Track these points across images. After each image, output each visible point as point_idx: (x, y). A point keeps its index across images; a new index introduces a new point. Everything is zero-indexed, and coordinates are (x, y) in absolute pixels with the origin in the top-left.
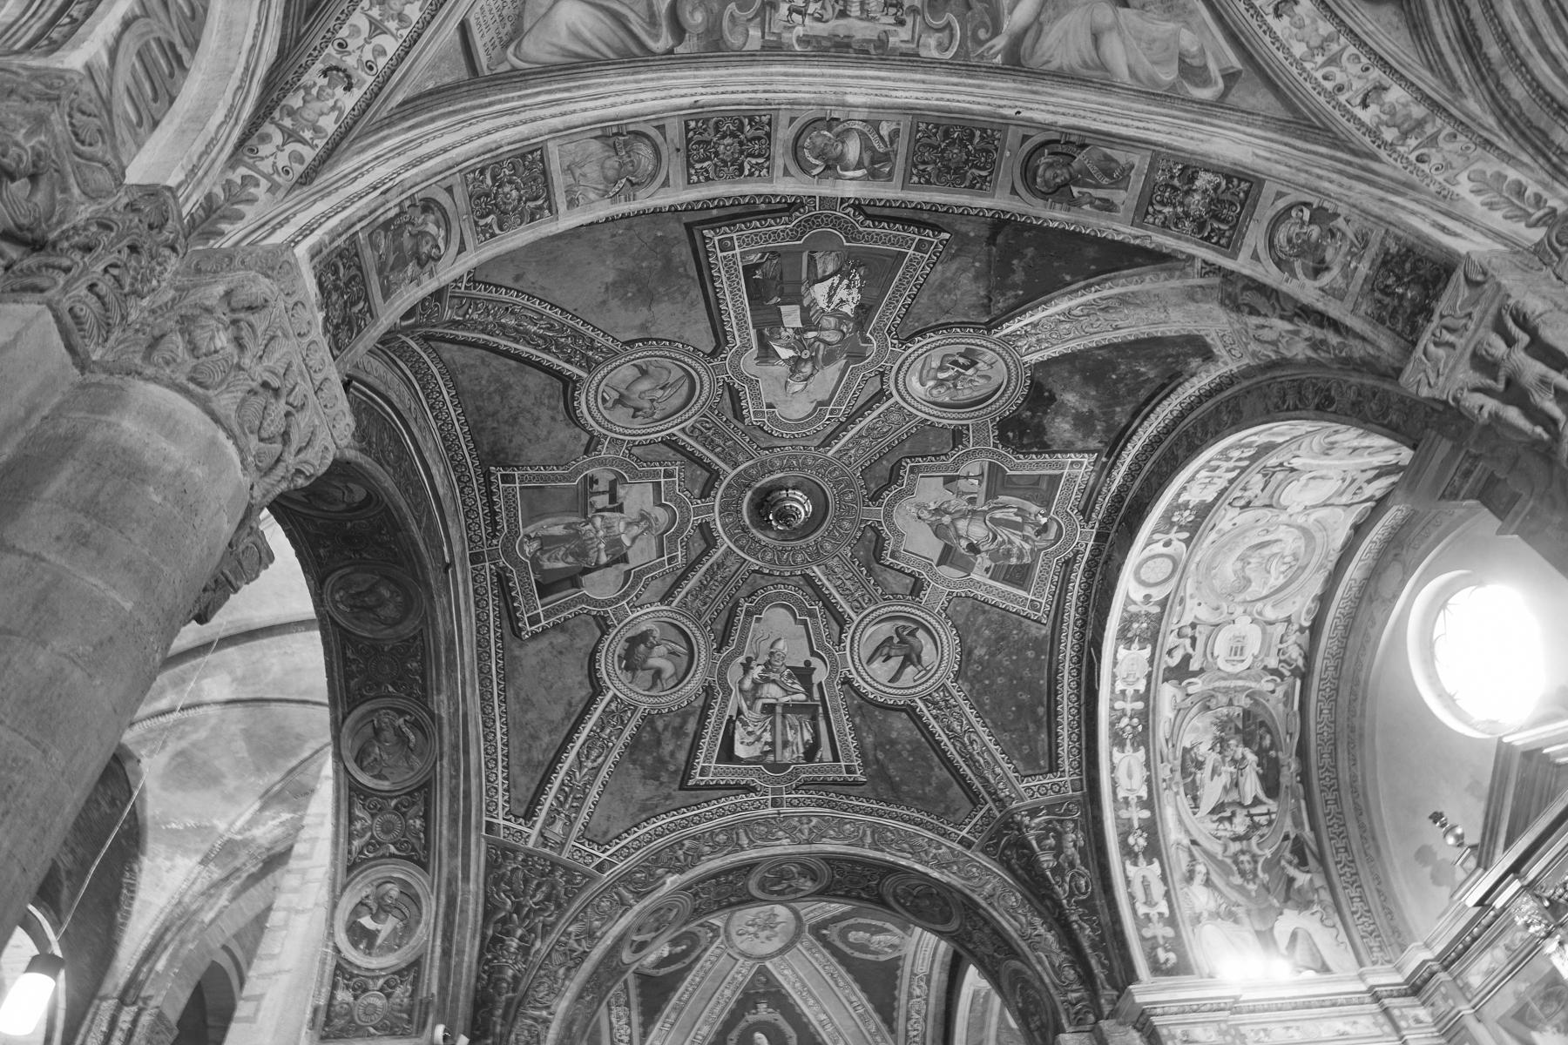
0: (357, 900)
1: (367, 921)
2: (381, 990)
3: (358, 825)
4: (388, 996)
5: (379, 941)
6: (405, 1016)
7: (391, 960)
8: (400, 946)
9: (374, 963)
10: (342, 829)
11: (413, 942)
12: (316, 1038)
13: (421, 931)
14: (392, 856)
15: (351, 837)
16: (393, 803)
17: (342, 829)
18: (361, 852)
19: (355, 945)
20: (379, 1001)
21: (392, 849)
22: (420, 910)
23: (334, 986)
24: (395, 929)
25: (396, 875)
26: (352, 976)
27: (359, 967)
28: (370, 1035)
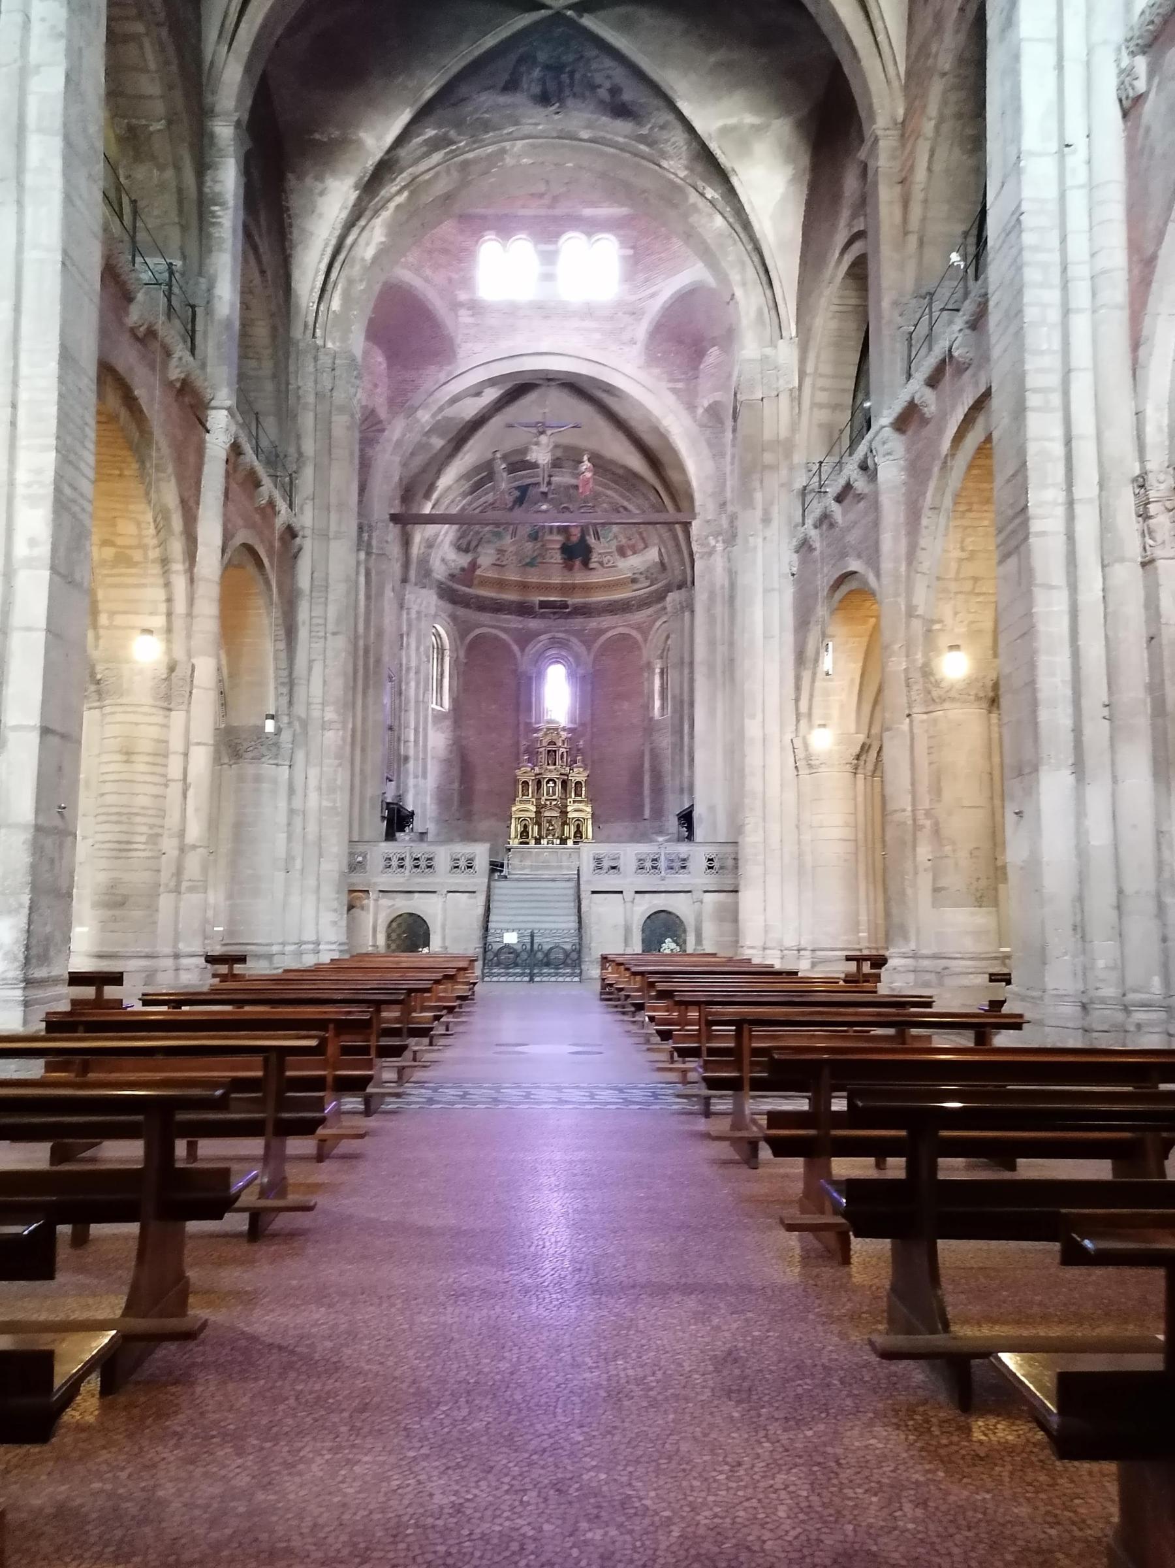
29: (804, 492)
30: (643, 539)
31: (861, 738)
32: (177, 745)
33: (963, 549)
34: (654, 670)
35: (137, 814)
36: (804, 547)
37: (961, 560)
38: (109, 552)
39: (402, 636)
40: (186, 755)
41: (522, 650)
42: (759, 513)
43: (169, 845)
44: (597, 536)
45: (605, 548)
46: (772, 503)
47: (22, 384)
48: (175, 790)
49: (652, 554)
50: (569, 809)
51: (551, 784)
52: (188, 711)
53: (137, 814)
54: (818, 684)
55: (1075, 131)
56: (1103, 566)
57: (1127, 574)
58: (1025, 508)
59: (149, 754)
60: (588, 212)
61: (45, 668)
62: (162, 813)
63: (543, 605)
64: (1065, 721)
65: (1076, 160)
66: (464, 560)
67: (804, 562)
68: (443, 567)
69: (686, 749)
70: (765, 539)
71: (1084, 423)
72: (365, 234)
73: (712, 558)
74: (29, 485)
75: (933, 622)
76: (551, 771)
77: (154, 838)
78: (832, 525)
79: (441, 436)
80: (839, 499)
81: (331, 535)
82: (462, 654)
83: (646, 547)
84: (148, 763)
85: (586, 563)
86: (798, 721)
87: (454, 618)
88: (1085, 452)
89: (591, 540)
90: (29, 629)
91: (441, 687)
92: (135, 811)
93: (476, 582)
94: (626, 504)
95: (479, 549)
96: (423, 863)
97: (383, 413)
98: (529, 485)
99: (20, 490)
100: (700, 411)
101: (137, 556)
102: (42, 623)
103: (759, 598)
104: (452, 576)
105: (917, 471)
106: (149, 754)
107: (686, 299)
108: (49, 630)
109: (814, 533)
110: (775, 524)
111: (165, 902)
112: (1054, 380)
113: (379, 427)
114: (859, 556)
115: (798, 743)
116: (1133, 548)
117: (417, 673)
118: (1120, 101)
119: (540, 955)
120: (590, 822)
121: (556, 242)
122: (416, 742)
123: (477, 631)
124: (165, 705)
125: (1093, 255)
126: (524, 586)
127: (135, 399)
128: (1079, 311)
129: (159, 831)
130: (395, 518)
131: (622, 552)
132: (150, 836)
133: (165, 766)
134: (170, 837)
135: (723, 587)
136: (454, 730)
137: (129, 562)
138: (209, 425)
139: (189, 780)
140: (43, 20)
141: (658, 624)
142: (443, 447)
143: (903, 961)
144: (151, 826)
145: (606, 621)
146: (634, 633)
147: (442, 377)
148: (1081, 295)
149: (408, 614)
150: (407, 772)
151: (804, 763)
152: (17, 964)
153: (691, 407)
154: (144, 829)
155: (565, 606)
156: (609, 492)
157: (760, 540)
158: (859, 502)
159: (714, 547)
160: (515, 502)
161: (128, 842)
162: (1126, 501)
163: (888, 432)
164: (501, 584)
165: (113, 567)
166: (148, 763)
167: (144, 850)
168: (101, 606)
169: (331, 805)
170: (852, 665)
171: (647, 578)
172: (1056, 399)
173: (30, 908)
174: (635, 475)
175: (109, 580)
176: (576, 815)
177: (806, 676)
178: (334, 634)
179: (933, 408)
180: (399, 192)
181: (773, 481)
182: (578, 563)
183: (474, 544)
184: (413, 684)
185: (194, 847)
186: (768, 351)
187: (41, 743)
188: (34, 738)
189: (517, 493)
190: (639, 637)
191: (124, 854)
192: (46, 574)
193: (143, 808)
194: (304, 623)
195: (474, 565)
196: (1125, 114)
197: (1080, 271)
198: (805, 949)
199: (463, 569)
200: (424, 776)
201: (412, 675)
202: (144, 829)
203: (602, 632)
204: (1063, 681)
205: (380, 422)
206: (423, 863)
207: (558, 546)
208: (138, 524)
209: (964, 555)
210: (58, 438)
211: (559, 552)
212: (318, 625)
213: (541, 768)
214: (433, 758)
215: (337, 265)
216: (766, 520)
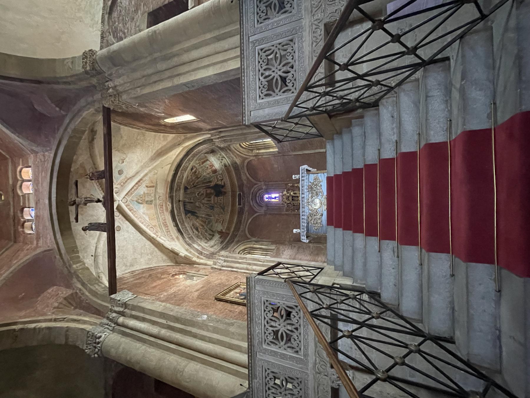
30: (204, 162)
34: (257, 153)
39: (232, 271)
41: (256, 212)
44: (210, 182)
45: (214, 178)
60: (11, 182)
63: (240, 204)
66: (217, 237)
68: (215, 247)
73: (120, 89)
82: (254, 239)
85: (223, 187)
87: (238, 241)
89: (212, 184)
91: (266, 249)
93: (228, 232)
94: (189, 168)
95: (214, 230)
97: (70, 292)
98: (185, 210)
100: (63, 113)
113: (74, 295)
123: (247, 232)
126: (232, 212)
136: (285, 245)
145: (244, 178)
149: (224, 267)
160: (194, 215)
164: (230, 222)
171: (222, 160)
182: (223, 190)
183: (211, 233)
184: (254, 267)
195: (220, 233)
199: (220, 238)
201: (250, 267)
203: (248, 178)
205: (72, 294)
207: (216, 198)
211: (218, 198)
214: (294, 259)
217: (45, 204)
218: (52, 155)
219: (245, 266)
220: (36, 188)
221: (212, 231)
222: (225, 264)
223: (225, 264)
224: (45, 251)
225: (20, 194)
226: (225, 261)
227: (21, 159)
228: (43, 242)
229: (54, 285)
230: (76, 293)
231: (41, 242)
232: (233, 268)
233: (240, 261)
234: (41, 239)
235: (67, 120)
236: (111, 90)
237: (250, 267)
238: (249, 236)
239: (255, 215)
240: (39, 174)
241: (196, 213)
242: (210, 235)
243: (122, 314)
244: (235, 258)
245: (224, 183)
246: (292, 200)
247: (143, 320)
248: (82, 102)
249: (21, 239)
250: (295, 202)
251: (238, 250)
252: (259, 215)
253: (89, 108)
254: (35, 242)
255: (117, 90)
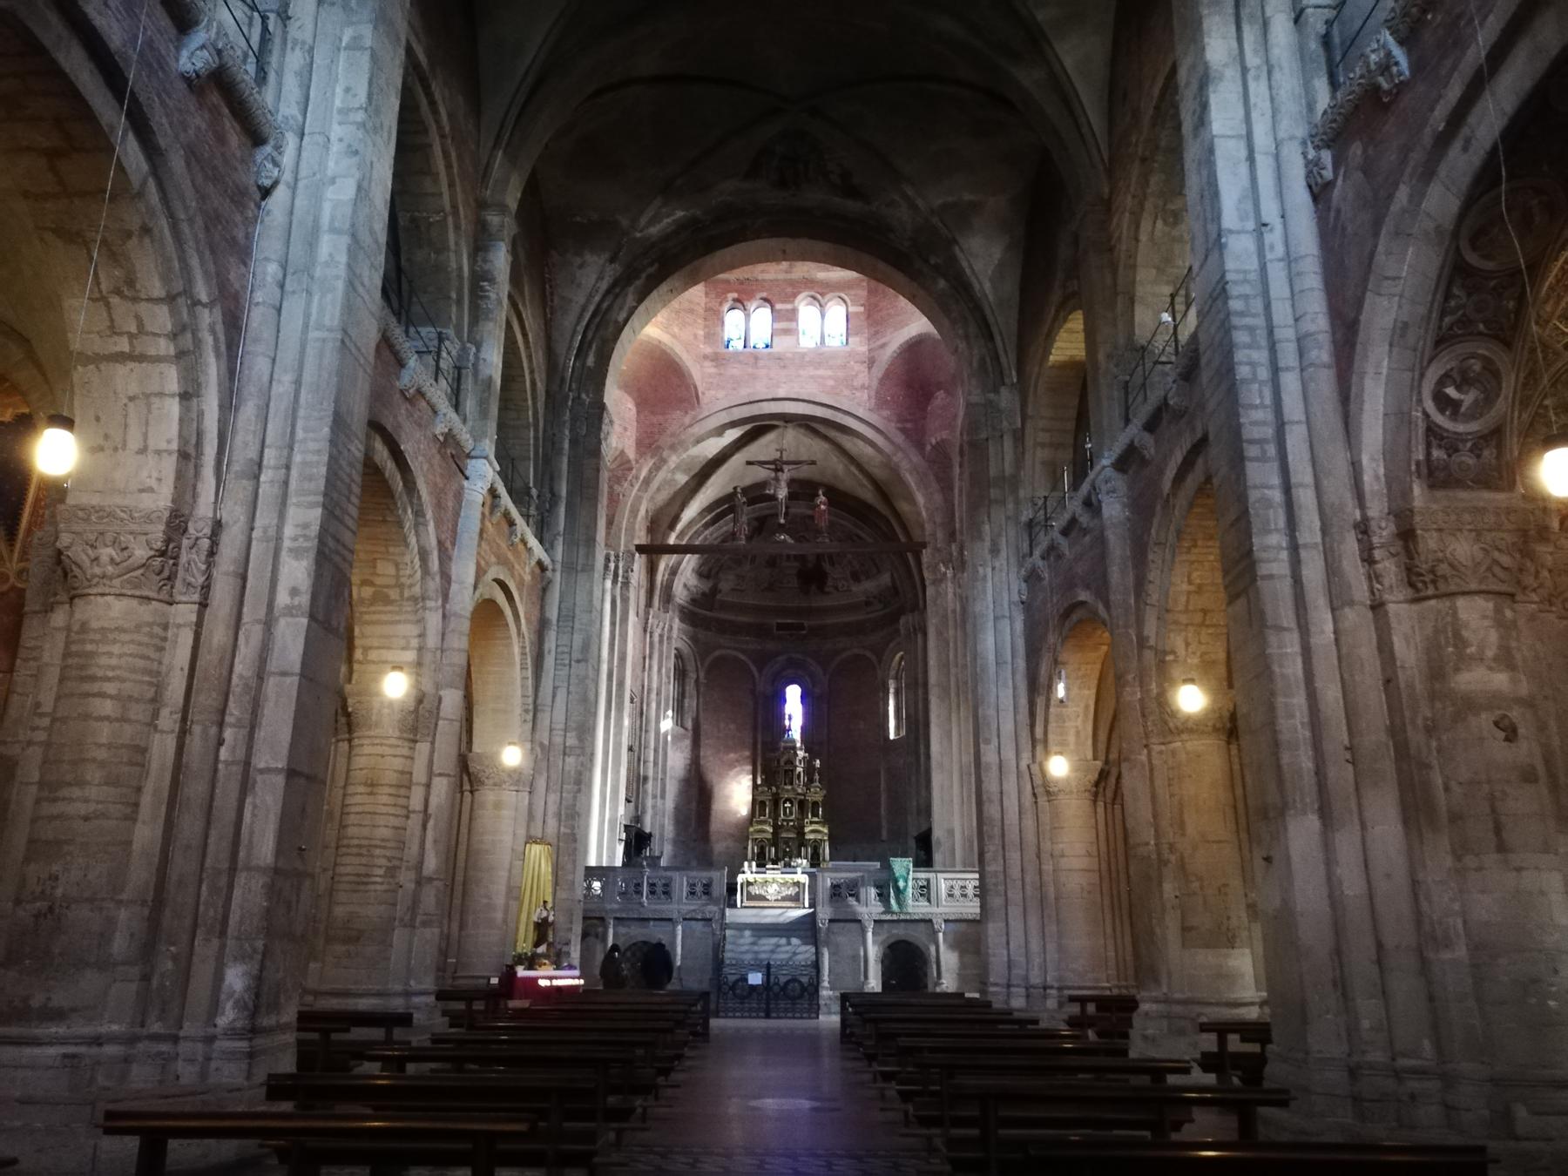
0: (1442, 372)
1: (1451, 391)
2: (1471, 451)
3: (1453, 303)
4: (1478, 456)
5: (1463, 409)
6: (1495, 474)
7: (1474, 426)
8: (1481, 415)
9: (1461, 428)
10: (1436, 305)
11: (1493, 413)
12: (1425, 487)
13: (1501, 405)
14: (1480, 334)
15: (1443, 314)
16: (1492, 283)
17: (1436, 305)
18: (1451, 328)
19: (1442, 411)
20: (1470, 461)
21: (1481, 326)
22: (1499, 384)
23: (1428, 446)
24: (1476, 401)
25: (1480, 352)
26: (1442, 438)
27: (1447, 431)
28: (1469, 487)
29: (1030, 525)
31: (1099, 764)
32: (420, 775)
33: (1190, 582)
35: (376, 846)
36: (1032, 578)
37: (1189, 593)
38: (367, 592)
39: (644, 658)
40: (428, 786)
41: (760, 671)
42: (987, 544)
43: (406, 878)
46: (999, 535)
47: (296, 446)
48: (415, 822)
49: (885, 579)
50: (807, 829)
51: (788, 805)
52: (433, 743)
53: (376, 846)
54: (1052, 710)
55: (1270, 211)
56: (1333, 610)
57: (1357, 618)
58: (1250, 552)
59: (391, 786)
61: (297, 712)
62: (401, 844)
63: (780, 627)
64: (1307, 764)
65: (1274, 238)
66: (705, 586)
67: (1031, 590)
69: (922, 768)
70: (993, 569)
71: (1302, 473)
72: (619, 301)
73: (943, 586)
74: (295, 539)
75: (1165, 653)
76: (788, 791)
77: (391, 871)
78: (1060, 557)
79: (685, 471)
80: (1065, 532)
81: (579, 568)
82: (702, 675)
83: (879, 572)
84: (390, 795)
85: (821, 589)
86: (1034, 747)
88: (1306, 498)
89: (827, 566)
90: (284, 674)
92: (378, 843)
94: (860, 532)
96: (659, 889)
97: (631, 454)
99: (287, 543)
100: (928, 448)
101: (394, 594)
102: (297, 668)
103: (991, 624)
104: (693, 601)
105: (1143, 508)
106: (391, 786)
107: (914, 348)
108: (302, 675)
109: (1040, 563)
110: (1003, 554)
111: (399, 936)
112: (1269, 432)
113: (627, 466)
114: (1087, 587)
115: (1035, 768)
116: (1360, 591)
117: (658, 694)
118: (1310, 187)
119: (776, 989)
120: (827, 844)
121: (793, 302)
122: (656, 764)
123: (717, 653)
124: (411, 736)
125: (1296, 320)
127: (401, 452)
128: (1287, 369)
129: (397, 863)
130: (641, 549)
131: (856, 577)
132: (388, 868)
133: (408, 798)
134: (408, 869)
135: (954, 611)
137: (387, 601)
138: (467, 473)
139: (430, 811)
140: (341, 140)
141: (891, 645)
142: (687, 483)
143: (1154, 1007)
144: (389, 859)
146: (868, 654)
147: (687, 420)
148: (1288, 355)
150: (645, 792)
151: (1045, 789)
152: (246, 1013)
153: (919, 445)
154: (383, 862)
155: (801, 627)
156: (842, 522)
157: (989, 570)
158: (1085, 535)
159: (945, 574)
161: (367, 875)
162: (1350, 546)
163: (1109, 472)
165: (371, 604)
166: (390, 795)
167: (382, 883)
168: (358, 642)
169: (568, 831)
170: (1087, 692)
172: (1272, 450)
173: (264, 955)
174: (869, 507)
175: (367, 617)
176: (811, 836)
177: (1040, 701)
178: (578, 661)
179: (1153, 451)
180: (651, 264)
181: (998, 515)
183: (713, 572)
184: (654, 705)
185: (430, 880)
186: (991, 396)
187: (287, 783)
188: (280, 780)
189: (756, 524)
190: (874, 658)
191: (362, 887)
192: (305, 621)
193: (383, 840)
194: (549, 652)
196: (1315, 198)
197: (1286, 334)
198: (1052, 987)
199: (704, 594)
200: (663, 797)
201: (653, 696)
202: (383, 862)
204: (1302, 724)
205: (629, 461)
206: (659, 889)
208: (397, 565)
209: (1192, 588)
210: (325, 495)
212: (563, 653)
213: (777, 788)
215: (593, 327)
216: (995, 551)
217: (778, 387)
218: (860, 413)
219: (655, 685)
220: (807, 359)
221: (717, 573)
222: (656, 639)
223: (656, 639)
224: (695, 387)
225: (797, 301)
226: (661, 636)
227: (862, 309)
228: (710, 376)
229: (637, 405)
230: (630, 469)
231: (710, 368)
232: (650, 657)
233: (664, 670)
234: (713, 370)
235: (916, 458)
236: (943, 569)
237: (653, 696)
238: (707, 663)
239: (754, 669)
240: (831, 368)
241: (760, 534)
242: (710, 570)
243: (615, 581)
244: (668, 658)
245: (828, 593)
246: (786, 771)
247: (613, 624)
248: (938, 498)
249: (714, 304)
250: (782, 773)
251: (680, 645)
252: (753, 676)
253: (927, 509)
254: (708, 350)
255: (941, 581)
